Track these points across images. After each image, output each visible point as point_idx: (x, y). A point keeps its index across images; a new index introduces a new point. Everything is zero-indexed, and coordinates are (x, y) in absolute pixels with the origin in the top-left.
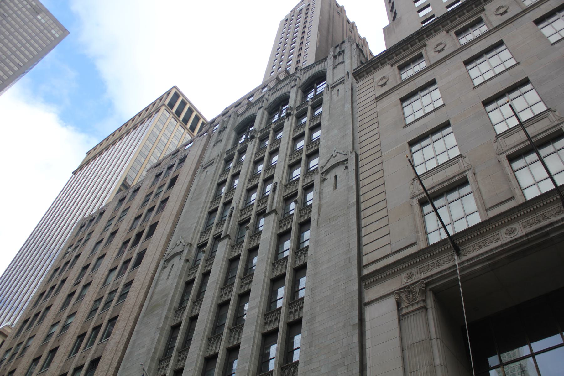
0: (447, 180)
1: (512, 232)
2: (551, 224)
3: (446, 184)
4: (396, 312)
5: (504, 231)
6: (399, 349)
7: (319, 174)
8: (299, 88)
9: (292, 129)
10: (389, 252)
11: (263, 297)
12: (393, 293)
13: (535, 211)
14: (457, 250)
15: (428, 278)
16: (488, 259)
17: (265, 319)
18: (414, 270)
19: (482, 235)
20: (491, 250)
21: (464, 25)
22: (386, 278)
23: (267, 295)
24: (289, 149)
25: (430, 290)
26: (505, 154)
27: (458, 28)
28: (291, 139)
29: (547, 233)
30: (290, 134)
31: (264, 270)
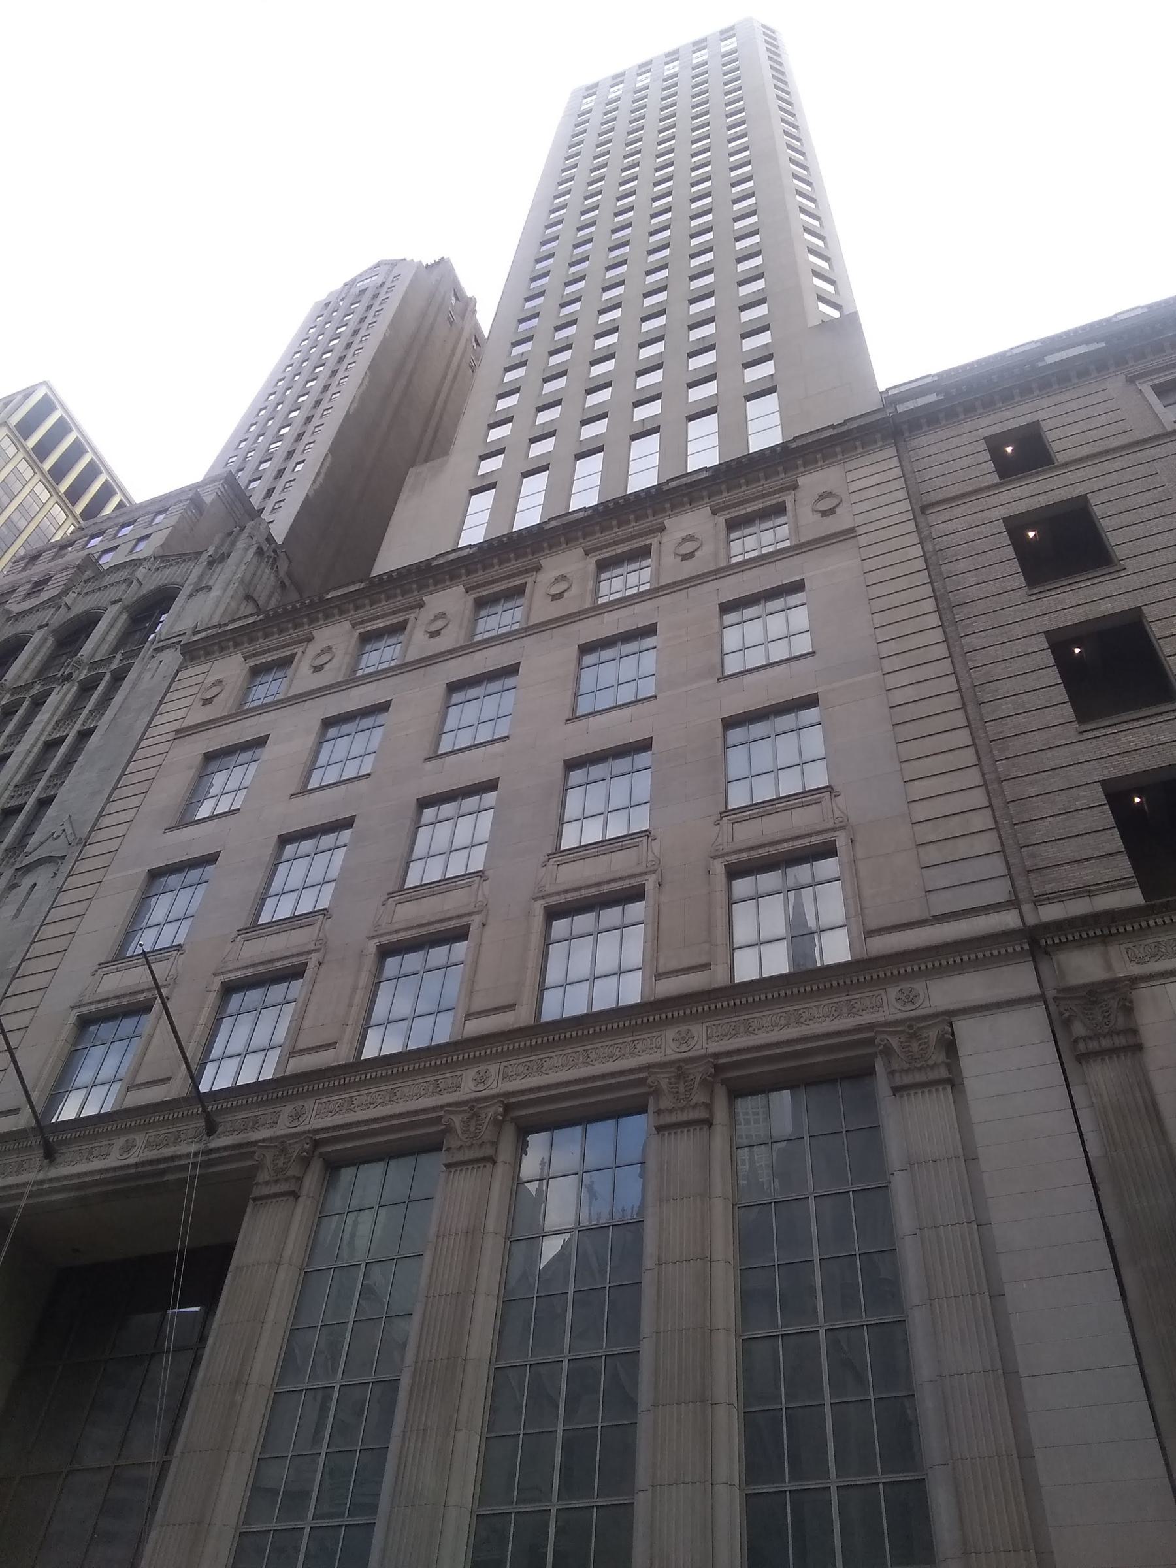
0: (131, 994)
1: (127, 1149)
2: (172, 1158)
3: (126, 1000)
5: (121, 1141)
7: (12, 871)
8: (126, 608)
9: (56, 718)
14: (50, 1154)
20: (79, 1175)
21: (380, 625)
24: (23, 770)
26: (221, 978)
27: (369, 627)
28: (40, 744)
29: (164, 1172)
30: (43, 730)
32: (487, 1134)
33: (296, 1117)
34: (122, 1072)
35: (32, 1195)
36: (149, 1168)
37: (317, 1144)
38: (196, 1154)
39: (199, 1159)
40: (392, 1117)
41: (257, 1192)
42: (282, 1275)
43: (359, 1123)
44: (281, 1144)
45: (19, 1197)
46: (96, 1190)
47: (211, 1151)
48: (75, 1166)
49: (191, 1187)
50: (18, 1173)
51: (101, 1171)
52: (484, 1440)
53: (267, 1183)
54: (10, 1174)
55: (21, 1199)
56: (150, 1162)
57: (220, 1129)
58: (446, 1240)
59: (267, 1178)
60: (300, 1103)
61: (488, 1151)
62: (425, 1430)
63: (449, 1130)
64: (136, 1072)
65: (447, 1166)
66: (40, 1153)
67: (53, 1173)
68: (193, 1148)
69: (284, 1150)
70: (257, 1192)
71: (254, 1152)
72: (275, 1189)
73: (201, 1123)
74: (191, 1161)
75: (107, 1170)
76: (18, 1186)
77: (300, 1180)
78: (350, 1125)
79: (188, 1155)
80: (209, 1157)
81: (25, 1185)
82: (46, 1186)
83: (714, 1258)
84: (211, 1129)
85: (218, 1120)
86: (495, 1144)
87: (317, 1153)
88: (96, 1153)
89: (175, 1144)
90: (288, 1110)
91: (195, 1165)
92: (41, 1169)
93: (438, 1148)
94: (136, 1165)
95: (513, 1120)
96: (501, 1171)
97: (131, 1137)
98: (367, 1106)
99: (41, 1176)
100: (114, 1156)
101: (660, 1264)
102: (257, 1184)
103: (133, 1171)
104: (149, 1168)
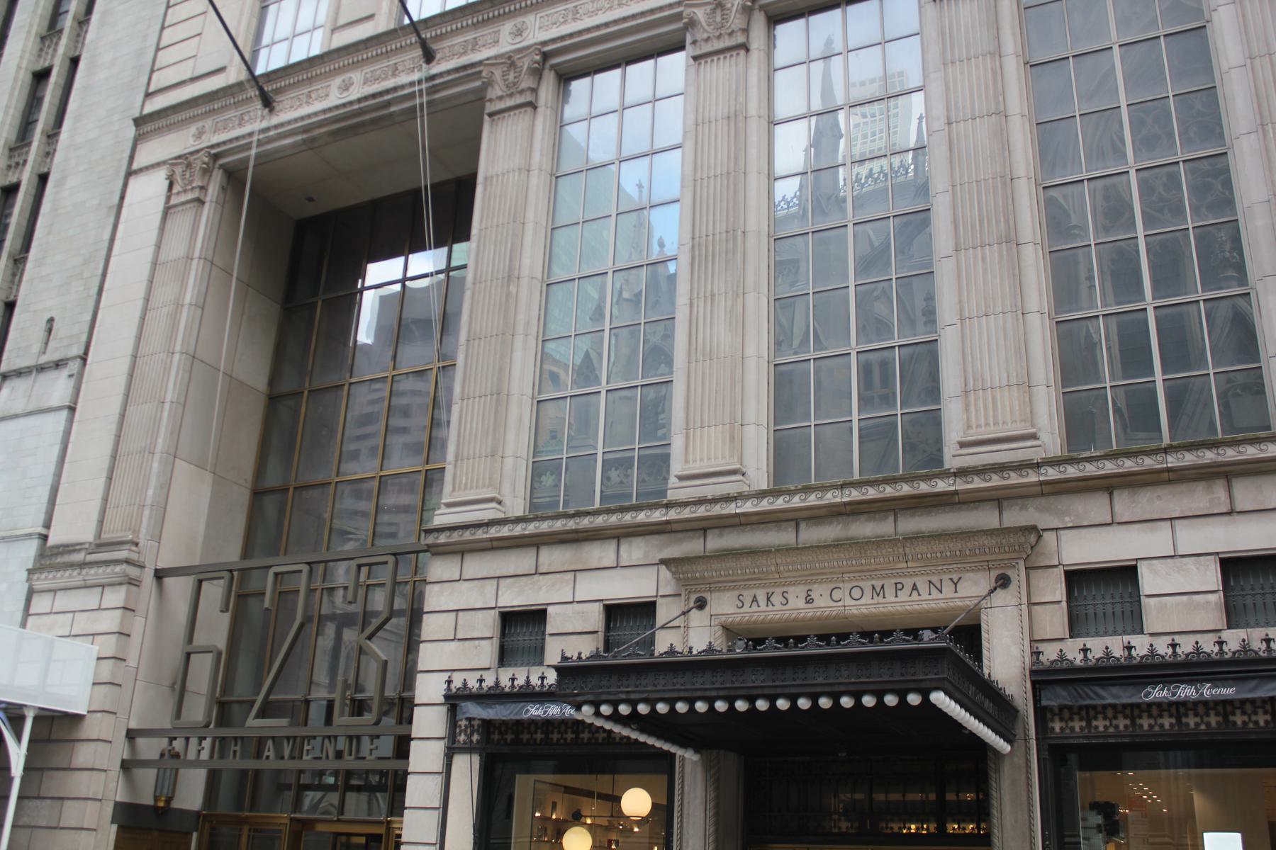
1: (346, 87)
2: (395, 89)
4: (163, 199)
5: (337, 81)
6: (148, 267)
10: (188, 76)
11: (11, 111)
12: (164, 163)
13: (387, 54)
15: (218, 145)
16: (305, 130)
17: (10, 157)
18: (208, 123)
19: (310, 81)
20: (302, 118)
22: (170, 128)
23: (22, 106)
25: (221, 166)
29: (388, 104)
31: (19, 54)
32: (736, 22)
33: (519, 32)
34: (321, 19)
35: (260, 143)
36: (372, 102)
37: (546, 56)
38: (420, 82)
39: (424, 86)
40: (624, 19)
41: (490, 108)
42: (534, 180)
43: (588, 30)
44: (509, 61)
45: (248, 147)
46: (323, 130)
47: (432, 78)
48: (297, 109)
49: (422, 109)
50: (240, 125)
51: (324, 111)
52: (772, 302)
53: (500, 98)
54: (233, 128)
55: (250, 148)
56: (374, 96)
57: (438, 56)
58: (706, 126)
59: (500, 93)
60: (520, 19)
61: (740, 39)
62: (713, 295)
63: (692, 24)
64: (336, 19)
65: (695, 58)
66: (258, 104)
67: (275, 120)
68: (416, 76)
69: (512, 65)
70: (490, 108)
71: (481, 72)
72: (510, 103)
73: (418, 52)
74: (417, 88)
75: (330, 110)
76: (243, 137)
77: (534, 91)
78: (580, 33)
79: (412, 84)
80: (434, 84)
81: (251, 134)
82: (272, 133)
83: (1010, 112)
84: (429, 57)
85: (434, 47)
86: (746, 31)
87: (547, 65)
88: (314, 96)
89: (394, 75)
90: (507, 27)
91: (421, 91)
92: (263, 117)
93: (680, 47)
94: (359, 100)
95: (762, 8)
96: (756, 55)
97: (346, 76)
98: (594, 13)
99: (264, 124)
100: (333, 95)
101: (949, 124)
102: (491, 100)
103: (356, 107)
104: (372, 102)
